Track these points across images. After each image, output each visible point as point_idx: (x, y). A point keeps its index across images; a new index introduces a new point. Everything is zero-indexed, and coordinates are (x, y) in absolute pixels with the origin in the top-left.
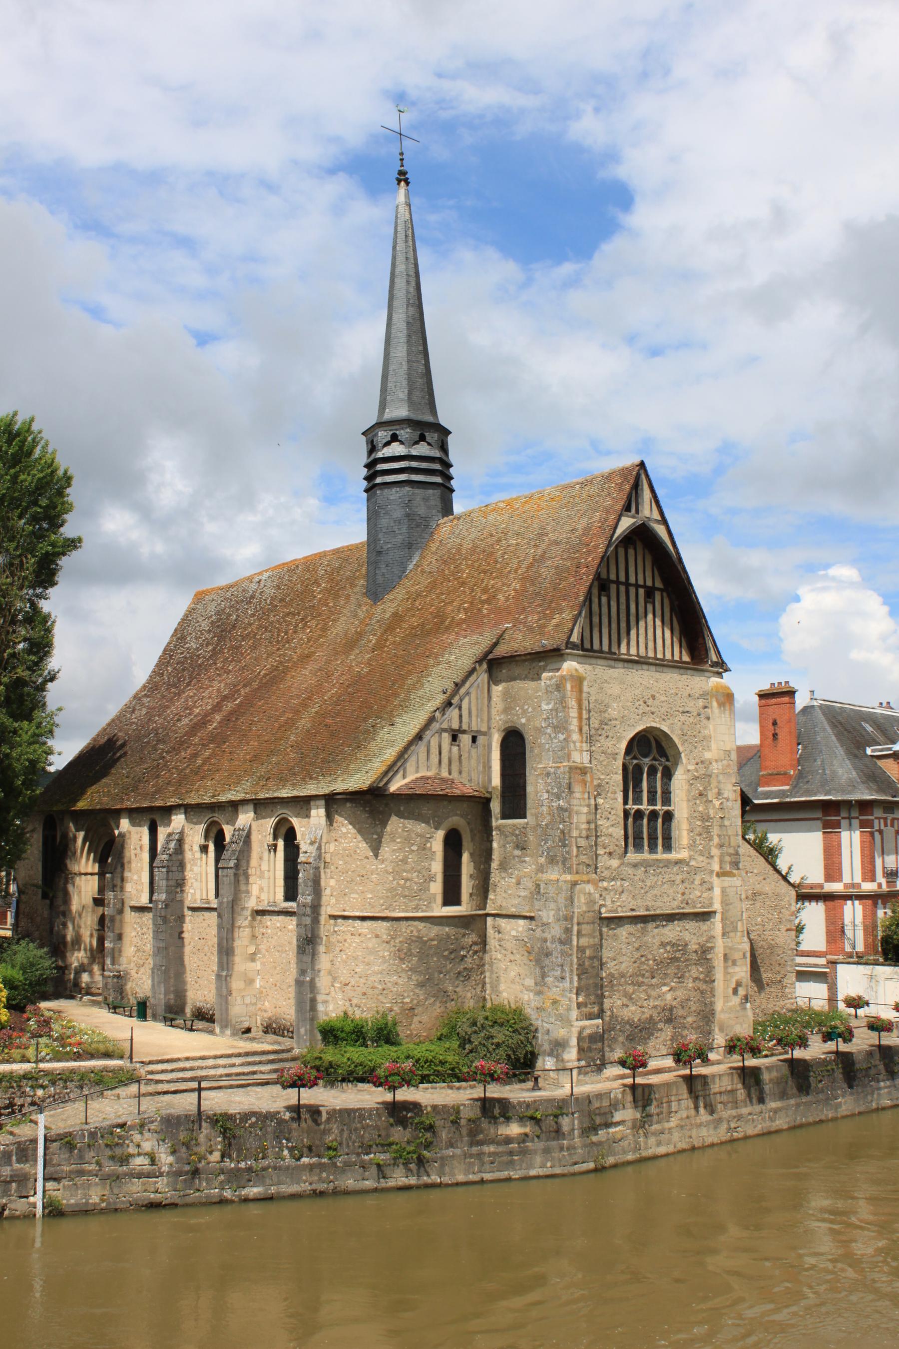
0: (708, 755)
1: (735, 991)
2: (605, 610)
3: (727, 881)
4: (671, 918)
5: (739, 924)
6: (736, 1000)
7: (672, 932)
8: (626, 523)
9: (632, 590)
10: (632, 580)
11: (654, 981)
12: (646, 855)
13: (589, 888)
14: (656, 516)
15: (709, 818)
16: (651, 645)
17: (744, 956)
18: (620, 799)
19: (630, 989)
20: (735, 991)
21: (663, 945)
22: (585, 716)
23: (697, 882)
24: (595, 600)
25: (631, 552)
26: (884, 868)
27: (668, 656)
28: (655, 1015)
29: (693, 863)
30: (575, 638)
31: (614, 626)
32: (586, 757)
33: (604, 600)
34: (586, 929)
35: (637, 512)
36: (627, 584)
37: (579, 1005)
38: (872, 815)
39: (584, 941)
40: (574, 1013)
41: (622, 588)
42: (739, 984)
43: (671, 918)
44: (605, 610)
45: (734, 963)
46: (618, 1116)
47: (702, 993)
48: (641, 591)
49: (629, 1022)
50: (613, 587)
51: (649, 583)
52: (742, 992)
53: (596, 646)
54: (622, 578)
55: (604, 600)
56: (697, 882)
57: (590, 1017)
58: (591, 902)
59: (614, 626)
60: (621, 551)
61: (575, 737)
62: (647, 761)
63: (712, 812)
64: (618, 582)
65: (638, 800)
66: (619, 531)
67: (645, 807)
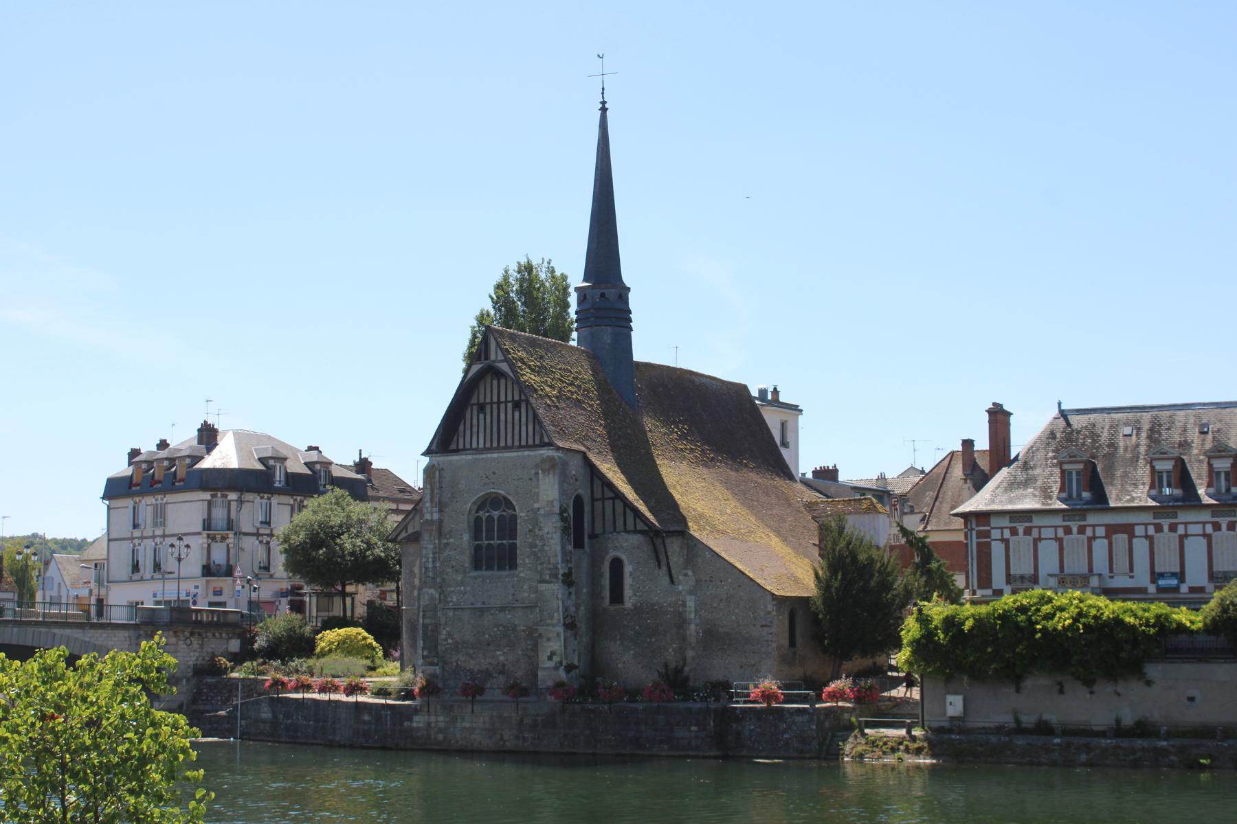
0: (536, 505)
1: (550, 658)
2: (482, 422)
3: (543, 587)
4: (502, 609)
5: (556, 615)
6: (551, 664)
7: (505, 617)
8: (476, 368)
9: (502, 406)
10: (503, 398)
11: (491, 648)
12: (496, 573)
13: (432, 591)
14: (500, 357)
15: (536, 546)
16: (516, 437)
17: (558, 635)
18: (466, 537)
19: (471, 651)
20: (550, 658)
21: (497, 626)
22: (436, 491)
23: (526, 587)
24: (475, 418)
25: (503, 381)
26: (1008, 575)
27: (531, 442)
28: (491, 668)
29: (522, 575)
30: (434, 447)
31: (488, 431)
32: (436, 516)
33: (481, 416)
34: (429, 614)
35: (486, 358)
36: (499, 403)
37: (424, 657)
38: (989, 525)
39: (427, 621)
40: (420, 662)
41: (495, 406)
42: (553, 654)
43: (502, 609)
44: (482, 422)
45: (549, 639)
46: (416, 718)
47: (530, 657)
48: (510, 405)
49: (471, 671)
50: (488, 408)
51: (517, 398)
52: (556, 659)
53: (474, 446)
54: (495, 399)
55: (481, 416)
56: (526, 587)
57: (432, 664)
58: (432, 598)
59: (488, 431)
60: (495, 382)
61: (428, 505)
62: (496, 514)
63: (539, 543)
64: (492, 403)
65: (490, 537)
66: (470, 375)
67: (496, 542)
